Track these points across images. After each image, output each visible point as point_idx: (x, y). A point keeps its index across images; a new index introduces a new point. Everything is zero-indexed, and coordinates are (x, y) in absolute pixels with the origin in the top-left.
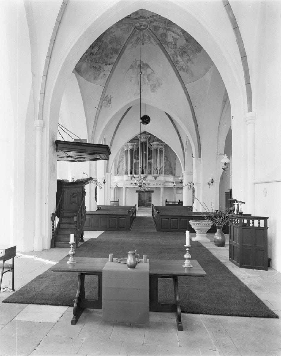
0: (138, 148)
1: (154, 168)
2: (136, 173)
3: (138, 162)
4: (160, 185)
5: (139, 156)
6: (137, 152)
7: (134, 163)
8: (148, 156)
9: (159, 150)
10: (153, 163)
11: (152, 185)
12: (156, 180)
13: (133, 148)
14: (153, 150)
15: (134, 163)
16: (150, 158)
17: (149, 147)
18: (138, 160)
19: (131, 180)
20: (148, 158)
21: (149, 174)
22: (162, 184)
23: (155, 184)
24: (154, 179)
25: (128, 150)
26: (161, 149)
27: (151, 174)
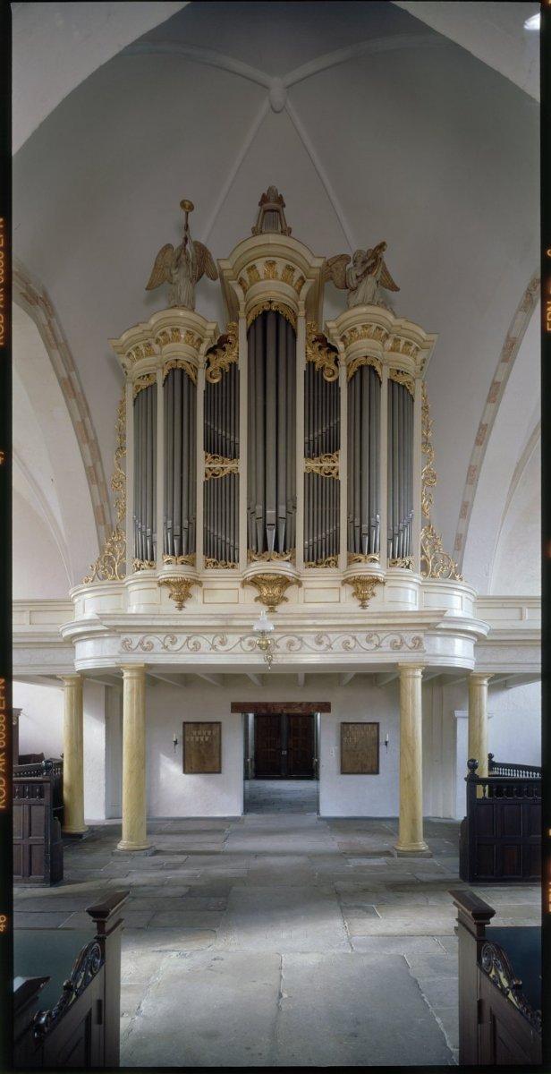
0: (234, 366)
2: (221, 554)
3: (233, 477)
4: (396, 647)
6: (222, 397)
7: (201, 479)
9: (391, 382)
11: (337, 646)
12: (364, 606)
13: (195, 369)
14: (343, 385)
15: (201, 479)
17: (310, 365)
19: (181, 607)
20: (307, 444)
22: (408, 637)
23: (362, 637)
24: (352, 605)
25: (153, 387)
26: (402, 380)
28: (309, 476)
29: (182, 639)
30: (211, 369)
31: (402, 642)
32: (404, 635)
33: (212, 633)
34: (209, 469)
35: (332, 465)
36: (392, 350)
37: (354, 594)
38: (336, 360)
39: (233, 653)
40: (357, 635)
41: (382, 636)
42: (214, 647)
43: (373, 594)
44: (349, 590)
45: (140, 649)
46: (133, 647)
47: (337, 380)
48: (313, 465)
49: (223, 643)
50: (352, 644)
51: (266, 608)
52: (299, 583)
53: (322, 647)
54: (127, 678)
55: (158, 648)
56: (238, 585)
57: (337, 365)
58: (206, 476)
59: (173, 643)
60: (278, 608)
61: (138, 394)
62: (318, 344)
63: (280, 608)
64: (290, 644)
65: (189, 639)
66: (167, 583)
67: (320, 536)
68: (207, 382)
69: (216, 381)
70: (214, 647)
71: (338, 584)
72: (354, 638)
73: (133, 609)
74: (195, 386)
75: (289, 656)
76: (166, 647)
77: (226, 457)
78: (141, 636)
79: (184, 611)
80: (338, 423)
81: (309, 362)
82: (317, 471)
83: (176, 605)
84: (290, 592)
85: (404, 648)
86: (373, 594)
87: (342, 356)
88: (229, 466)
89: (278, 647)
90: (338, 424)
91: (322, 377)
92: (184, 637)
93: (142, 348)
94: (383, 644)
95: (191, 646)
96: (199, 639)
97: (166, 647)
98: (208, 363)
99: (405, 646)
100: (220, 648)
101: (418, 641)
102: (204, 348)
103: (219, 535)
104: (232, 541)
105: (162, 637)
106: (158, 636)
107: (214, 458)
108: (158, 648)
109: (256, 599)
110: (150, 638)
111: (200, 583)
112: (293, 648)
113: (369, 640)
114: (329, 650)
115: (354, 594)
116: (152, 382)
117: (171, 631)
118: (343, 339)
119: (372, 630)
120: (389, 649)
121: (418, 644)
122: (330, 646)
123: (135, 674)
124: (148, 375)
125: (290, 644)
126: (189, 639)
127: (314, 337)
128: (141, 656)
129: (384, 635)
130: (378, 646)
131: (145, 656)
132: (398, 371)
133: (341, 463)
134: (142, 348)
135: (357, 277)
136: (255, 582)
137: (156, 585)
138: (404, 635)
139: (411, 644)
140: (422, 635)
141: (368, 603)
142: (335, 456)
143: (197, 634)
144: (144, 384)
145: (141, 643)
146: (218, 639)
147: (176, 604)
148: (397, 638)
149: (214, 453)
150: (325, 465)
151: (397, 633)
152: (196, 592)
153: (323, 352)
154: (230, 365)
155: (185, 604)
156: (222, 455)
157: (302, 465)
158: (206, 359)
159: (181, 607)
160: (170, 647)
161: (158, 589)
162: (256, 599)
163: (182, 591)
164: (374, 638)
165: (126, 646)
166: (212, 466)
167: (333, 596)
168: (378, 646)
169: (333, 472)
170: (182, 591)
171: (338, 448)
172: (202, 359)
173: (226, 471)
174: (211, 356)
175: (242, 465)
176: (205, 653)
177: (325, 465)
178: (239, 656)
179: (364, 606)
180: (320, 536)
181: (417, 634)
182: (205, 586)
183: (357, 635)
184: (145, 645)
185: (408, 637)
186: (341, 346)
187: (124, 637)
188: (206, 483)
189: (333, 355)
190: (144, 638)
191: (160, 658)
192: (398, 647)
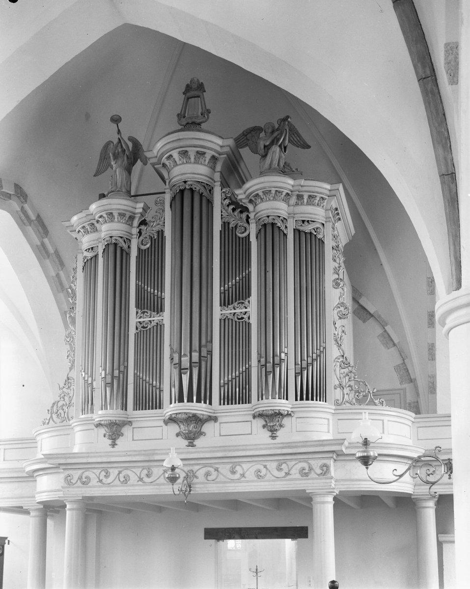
0: (161, 233)
1: (259, 355)
3: (160, 327)
4: (304, 474)
5: (162, 290)
8: (223, 281)
9: (297, 232)
10: (254, 321)
11: (250, 475)
12: (273, 437)
13: (128, 241)
14: (253, 239)
16: (240, 294)
17: (225, 225)
18: (160, 309)
19: (114, 445)
21: (228, 399)
22: (316, 464)
23: (273, 466)
26: (308, 228)
27: (245, 399)
28: (224, 321)
29: (114, 473)
30: (141, 238)
31: (311, 469)
32: (312, 462)
33: (139, 467)
34: (140, 322)
35: (244, 310)
36: (297, 204)
37: (264, 427)
38: (248, 217)
39: (157, 484)
40: (268, 464)
41: (291, 464)
42: (141, 479)
43: (281, 426)
44: (260, 422)
45: (79, 483)
46: (74, 482)
47: (249, 235)
48: (228, 311)
49: (148, 476)
50: (264, 471)
51: (186, 442)
52: (215, 419)
53: (237, 476)
54: (70, 510)
55: (94, 482)
56: (162, 424)
57: (248, 222)
58: (137, 329)
59: (107, 476)
60: (196, 442)
61: (85, 263)
62: (232, 207)
63: (197, 442)
64: (208, 474)
65: (120, 473)
66: (99, 425)
67: (234, 374)
68: (139, 249)
69: (148, 246)
70: (141, 479)
71: (250, 418)
72: (265, 467)
73: (76, 450)
74: (128, 254)
75: (207, 485)
76: (101, 481)
77: (154, 311)
78: (80, 472)
79: (117, 448)
80: (250, 273)
81: (224, 223)
82: (231, 317)
83: (110, 443)
84: (207, 428)
85: (313, 475)
86: (281, 426)
87: (252, 215)
88: (156, 319)
89: (197, 477)
90: (249, 274)
91: (236, 235)
92: (116, 471)
93: (88, 227)
94: (291, 472)
95: (122, 479)
96: (129, 472)
97: (101, 481)
98: (140, 233)
99: (313, 472)
100: (146, 480)
101: (325, 468)
102: (136, 223)
103: (148, 379)
104: (158, 384)
105: (97, 472)
106: (95, 471)
107: (144, 313)
108: (94, 482)
109: (178, 435)
110: (87, 474)
111: (130, 423)
112: (210, 478)
113: (279, 469)
114: (243, 479)
115: (264, 427)
116: (95, 254)
117: (105, 468)
118: (251, 201)
119: (284, 457)
120: (298, 476)
121: (325, 469)
122: (243, 475)
123: (75, 506)
124: (92, 248)
125: (208, 474)
126: (120, 473)
127: (227, 201)
128: (80, 489)
129: (294, 463)
130: (287, 474)
131: (83, 489)
132: (303, 221)
133: (252, 308)
134: (88, 227)
135: (265, 146)
136: (172, 420)
137: (93, 427)
138: (312, 462)
139: (319, 471)
140: (331, 463)
141: (278, 433)
142: (247, 303)
143: (127, 468)
144: (89, 255)
145: (80, 478)
146: (145, 472)
147: (110, 442)
148: (304, 465)
149: (144, 309)
150: (238, 311)
151: (305, 460)
152: (126, 430)
153: (236, 213)
154: (158, 232)
155: (118, 442)
156: (151, 310)
157: (218, 312)
158: (138, 230)
159: (114, 445)
160: (104, 480)
161: (96, 429)
162: (178, 435)
163: (115, 430)
164: (284, 466)
165: (68, 481)
166: (141, 320)
167: (245, 428)
168: (287, 474)
169: (245, 316)
170: (115, 430)
171: (249, 295)
172: (135, 231)
173: (153, 324)
174: (143, 227)
175: (166, 317)
176: (133, 485)
177: (238, 311)
178: (163, 487)
179: (273, 437)
180: (234, 374)
181: (325, 461)
182: (134, 425)
183: (268, 464)
184: (84, 480)
185: (316, 464)
186: (251, 207)
188: (137, 335)
189: (244, 215)
190: (83, 473)
191: (96, 491)
192: (306, 475)
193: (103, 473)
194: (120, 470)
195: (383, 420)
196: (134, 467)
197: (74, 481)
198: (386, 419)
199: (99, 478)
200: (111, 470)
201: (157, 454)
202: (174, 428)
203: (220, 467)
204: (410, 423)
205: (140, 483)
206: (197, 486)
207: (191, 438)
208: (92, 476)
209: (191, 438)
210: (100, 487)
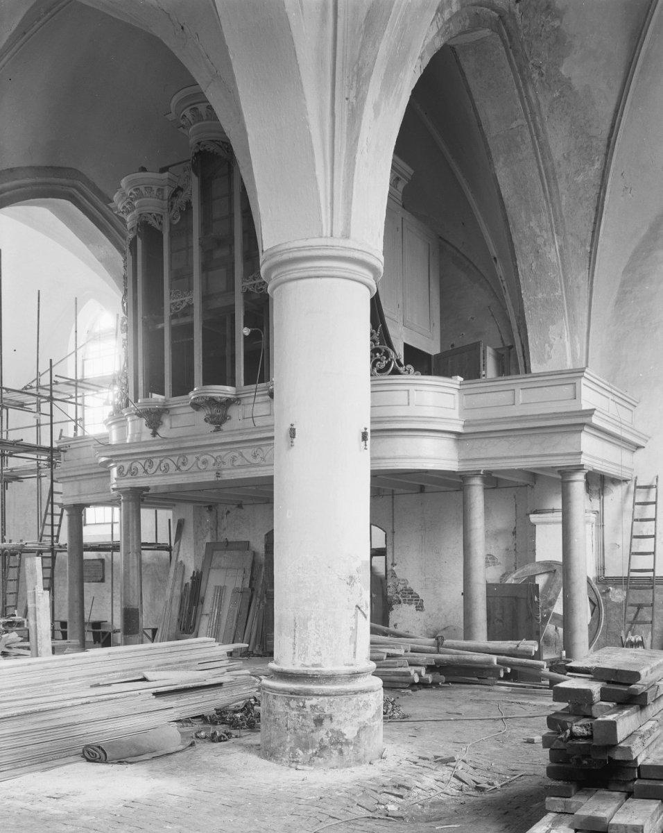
19: (154, 434)
33: (175, 455)
39: (191, 473)
42: (178, 468)
45: (129, 475)
51: (213, 427)
53: (258, 460)
58: (171, 311)
63: (224, 427)
65: (161, 462)
84: (234, 411)
88: (187, 299)
89: (224, 463)
100: (183, 468)
105: (143, 462)
110: (135, 464)
125: (233, 459)
126: (161, 462)
145: (130, 469)
146: (181, 460)
173: (184, 305)
187: (119, 464)
193: (148, 464)
194: (161, 459)
195: (408, 391)
196: (172, 456)
197: (125, 473)
198: (411, 388)
199: (144, 468)
200: (154, 460)
201: (186, 441)
202: (202, 415)
203: (244, 451)
204: (455, 392)
205: (178, 471)
206: (224, 472)
207: (218, 421)
208: (139, 467)
209: (218, 421)
210: (146, 477)
